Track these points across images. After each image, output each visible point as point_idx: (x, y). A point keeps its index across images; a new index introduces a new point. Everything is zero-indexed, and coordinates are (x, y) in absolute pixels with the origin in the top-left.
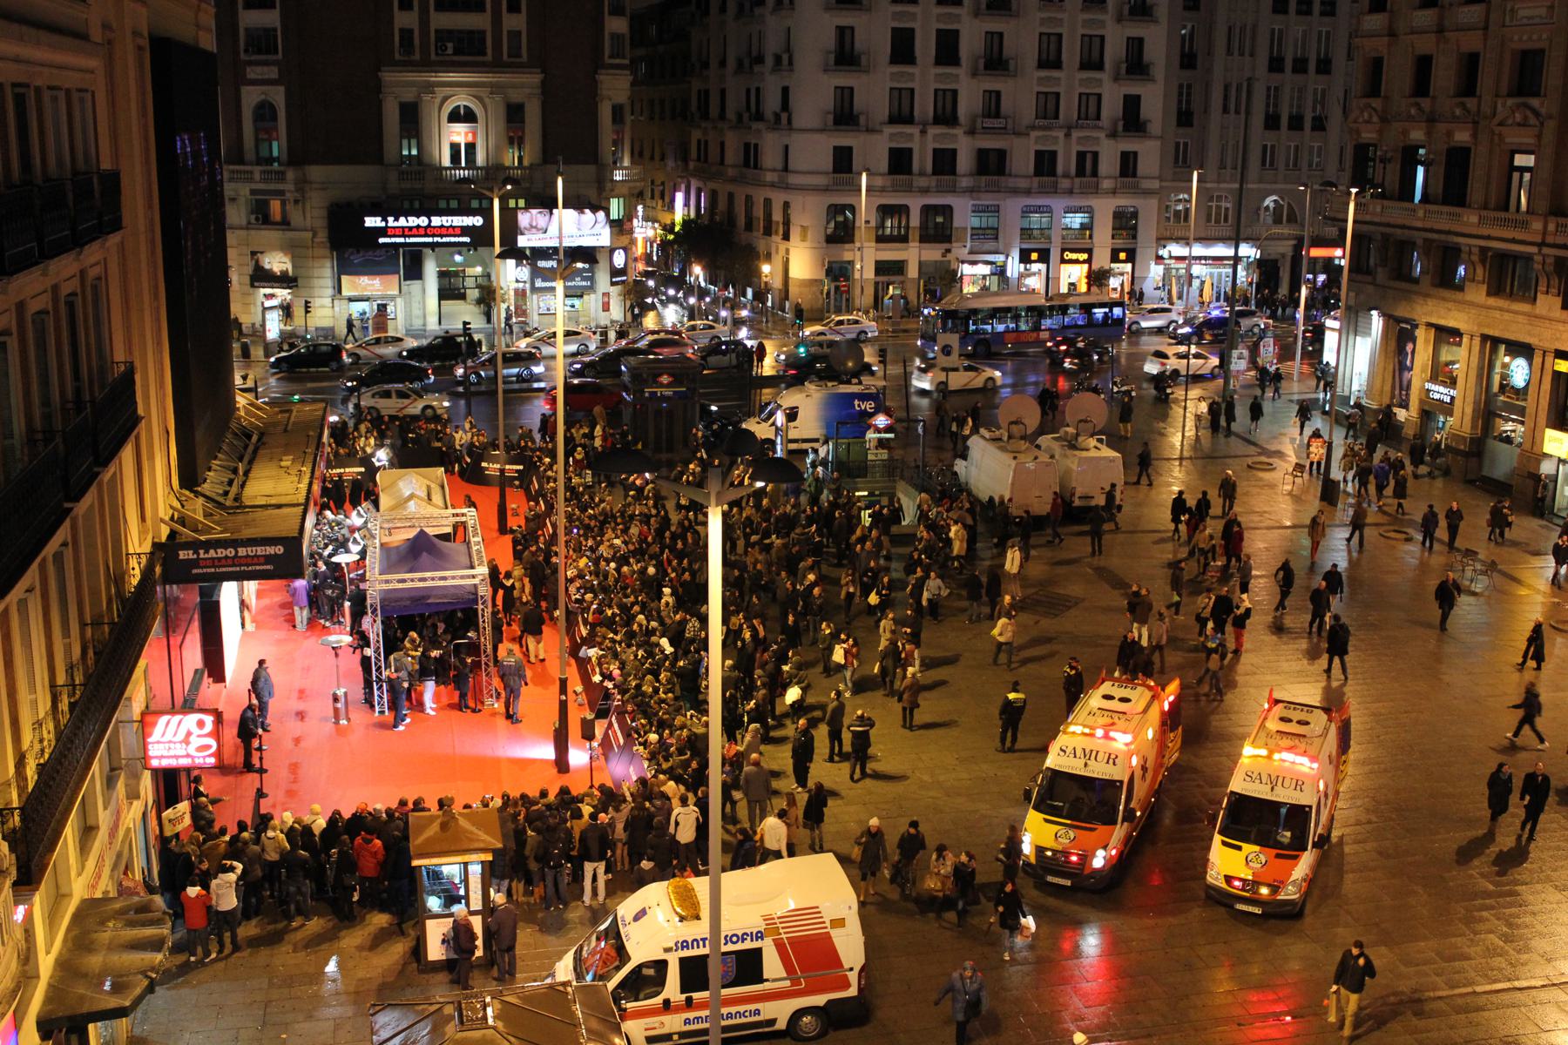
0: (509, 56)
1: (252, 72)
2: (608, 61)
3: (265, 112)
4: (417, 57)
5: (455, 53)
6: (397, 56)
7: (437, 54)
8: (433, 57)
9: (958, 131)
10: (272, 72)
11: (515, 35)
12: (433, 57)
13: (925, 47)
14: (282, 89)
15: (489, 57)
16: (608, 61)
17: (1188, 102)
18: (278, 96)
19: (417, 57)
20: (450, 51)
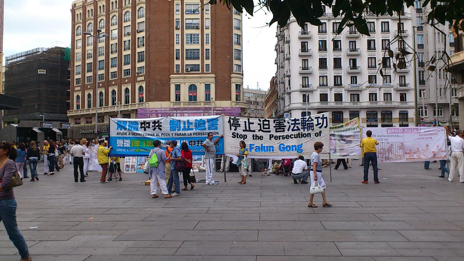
0: (206, 71)
1: (139, 79)
2: (234, 72)
3: (141, 88)
4: (180, 72)
5: (191, 71)
6: (175, 72)
7: (186, 71)
8: (185, 72)
9: (343, 89)
10: (142, 78)
11: (208, 65)
12: (185, 72)
13: (330, 64)
14: (145, 82)
15: (200, 72)
16: (234, 72)
17: (423, 77)
18: (144, 86)
19: (180, 72)
20: (189, 70)
